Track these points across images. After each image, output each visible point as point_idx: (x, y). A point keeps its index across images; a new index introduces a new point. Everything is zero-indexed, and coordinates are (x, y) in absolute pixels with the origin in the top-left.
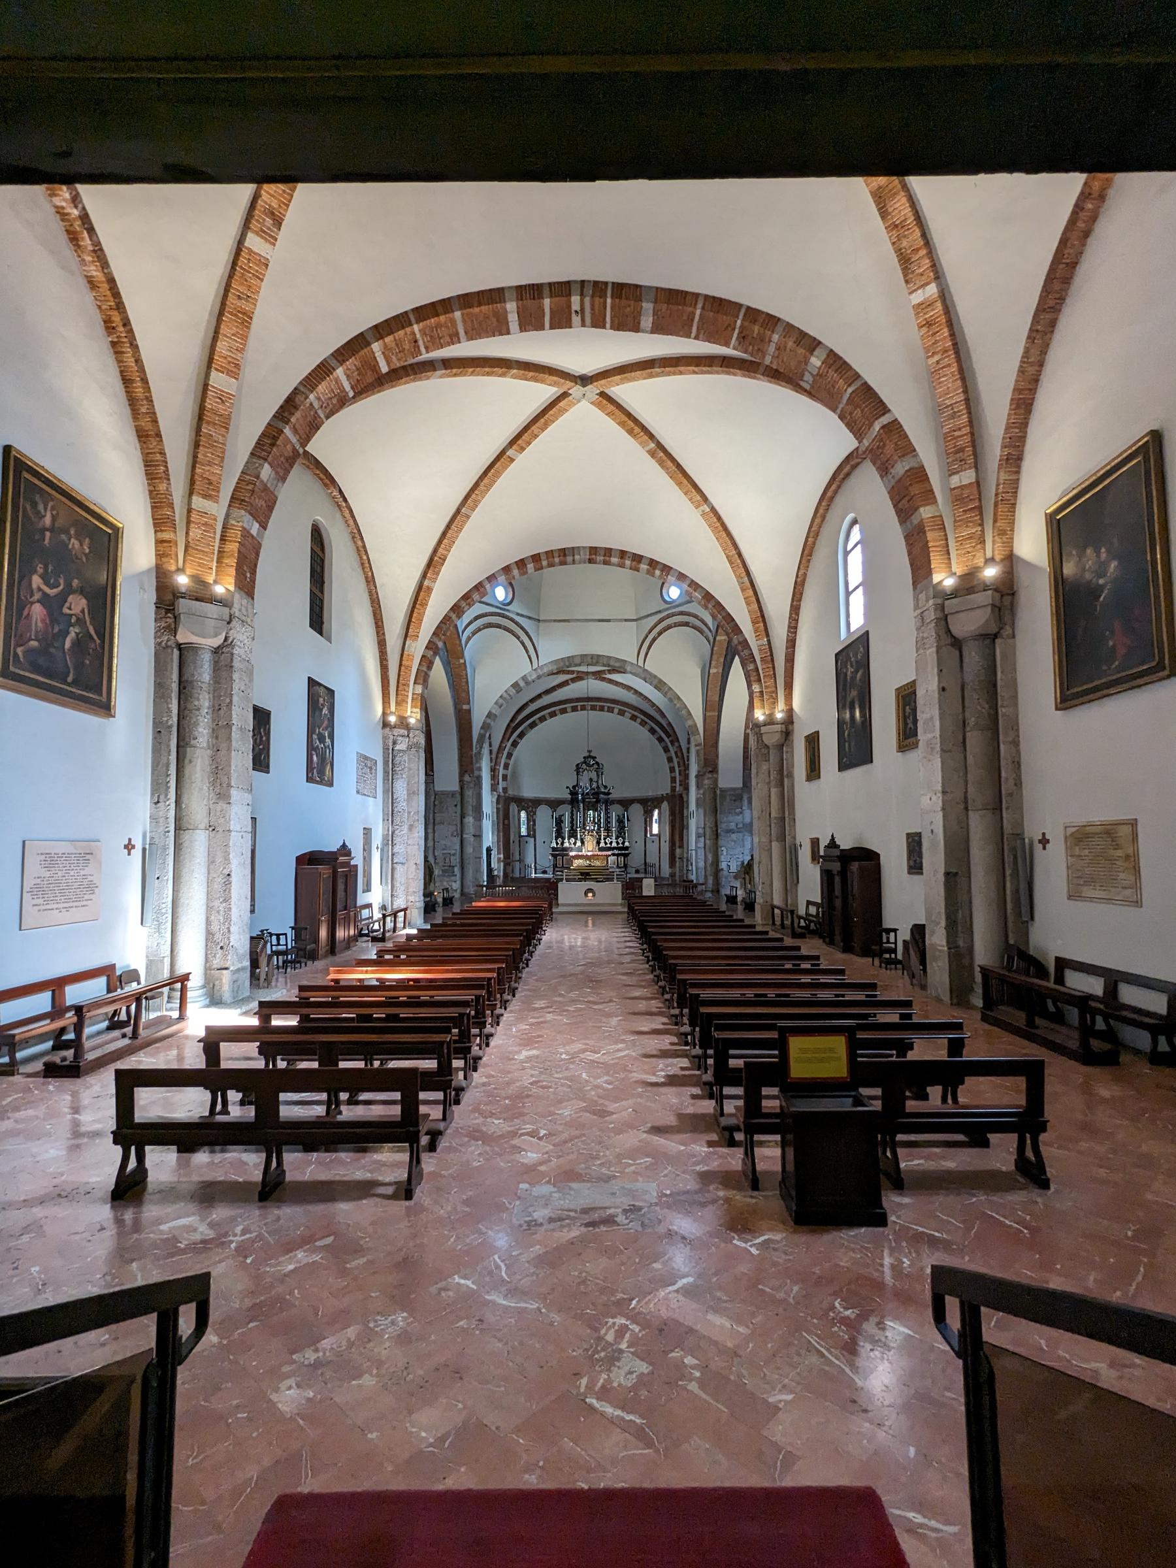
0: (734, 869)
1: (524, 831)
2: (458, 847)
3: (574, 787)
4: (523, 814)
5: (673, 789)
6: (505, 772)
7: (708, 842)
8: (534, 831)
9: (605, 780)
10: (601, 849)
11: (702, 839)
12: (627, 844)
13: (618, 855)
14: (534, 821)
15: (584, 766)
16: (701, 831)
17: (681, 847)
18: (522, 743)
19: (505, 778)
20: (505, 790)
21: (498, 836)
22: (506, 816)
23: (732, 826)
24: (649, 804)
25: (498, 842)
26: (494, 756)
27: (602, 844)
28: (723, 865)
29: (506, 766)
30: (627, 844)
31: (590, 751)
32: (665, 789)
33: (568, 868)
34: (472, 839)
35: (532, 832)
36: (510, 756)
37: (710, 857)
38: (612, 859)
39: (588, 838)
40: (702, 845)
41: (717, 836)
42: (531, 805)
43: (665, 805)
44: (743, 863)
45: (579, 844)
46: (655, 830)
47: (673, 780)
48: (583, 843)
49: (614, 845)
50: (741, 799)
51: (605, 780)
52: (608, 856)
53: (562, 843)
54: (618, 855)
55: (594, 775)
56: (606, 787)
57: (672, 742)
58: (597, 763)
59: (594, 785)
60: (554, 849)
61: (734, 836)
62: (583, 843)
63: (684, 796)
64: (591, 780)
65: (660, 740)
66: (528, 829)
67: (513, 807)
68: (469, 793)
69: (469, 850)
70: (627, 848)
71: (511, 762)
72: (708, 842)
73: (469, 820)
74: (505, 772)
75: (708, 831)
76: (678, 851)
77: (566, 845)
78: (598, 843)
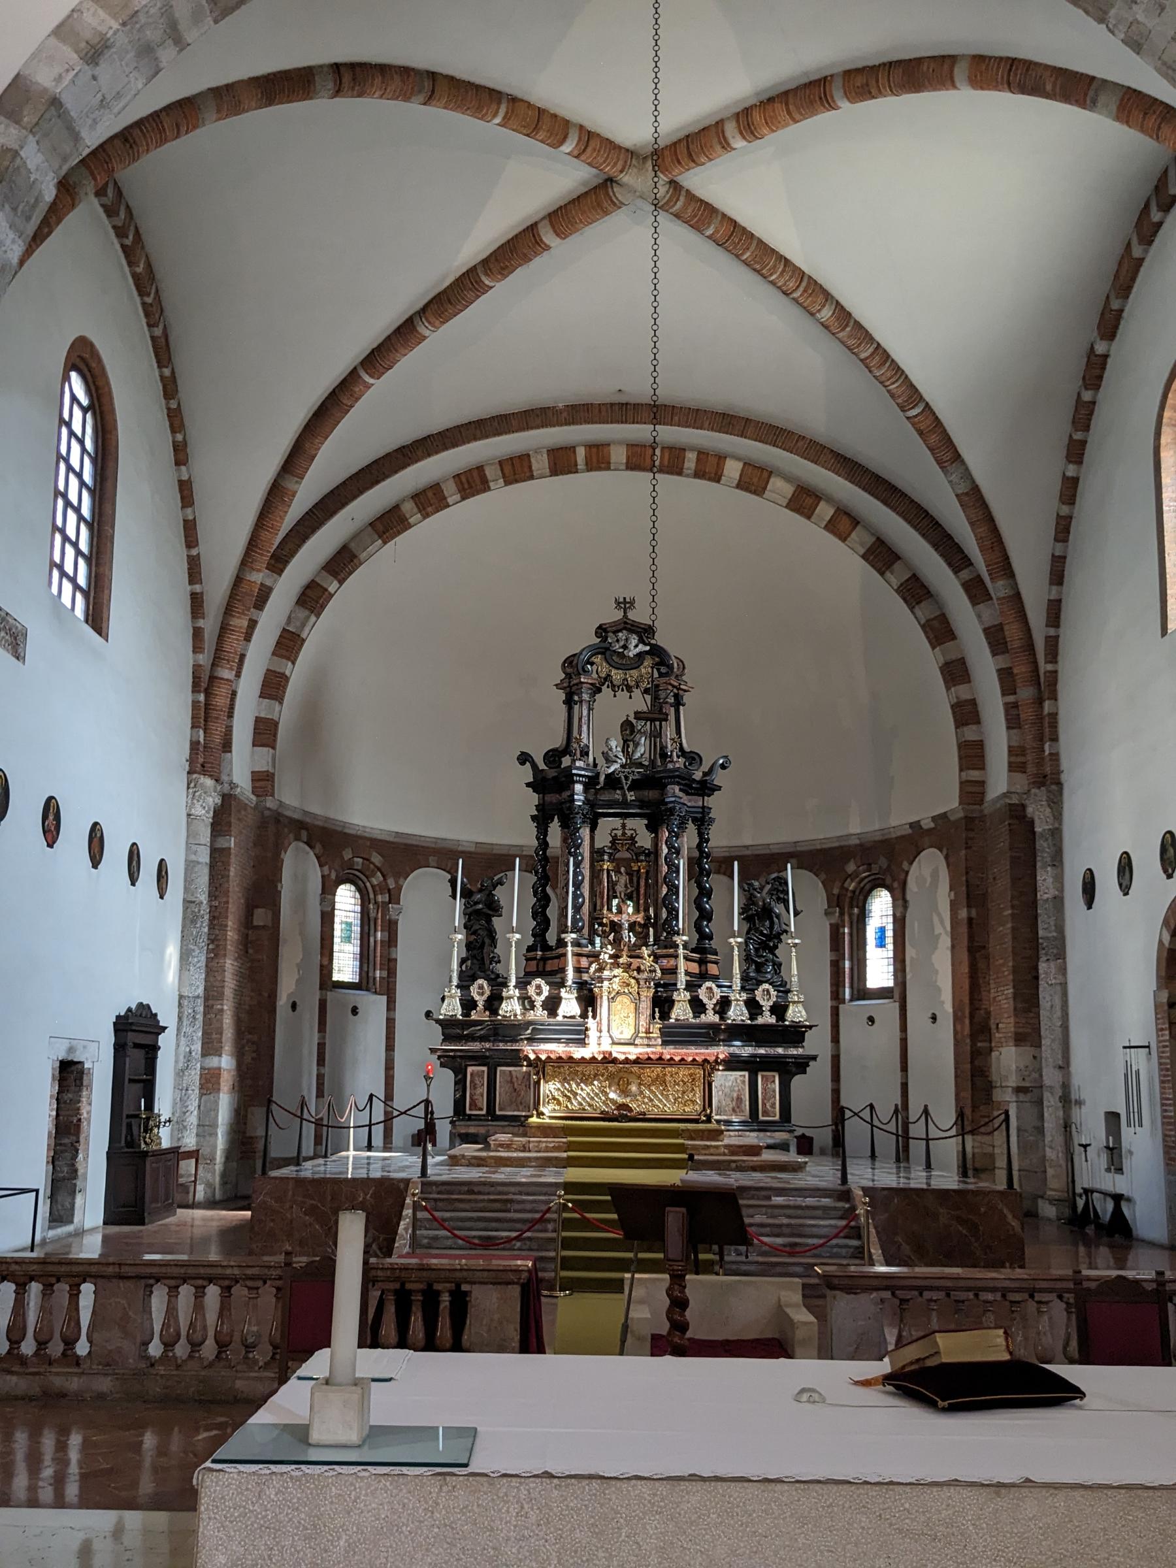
1: (345, 967)
3: (552, 757)
4: (346, 900)
6: (268, 709)
8: (390, 966)
10: (671, 1036)
13: (753, 1066)
14: (391, 928)
15: (600, 667)
17: (1029, 1036)
18: (346, 596)
19: (265, 732)
20: (263, 781)
21: (212, 971)
22: (263, 891)
25: (212, 995)
26: (210, 625)
27: (681, 1011)
29: (274, 686)
31: (625, 604)
32: (935, 794)
33: (518, 1124)
35: (379, 969)
36: (289, 644)
38: (729, 1083)
39: (613, 980)
42: (379, 865)
45: (570, 1006)
46: (879, 971)
48: (588, 1001)
49: (738, 1013)
51: (692, 731)
52: (709, 1067)
53: (493, 1003)
54: (753, 1066)
57: (976, 591)
58: (657, 652)
59: (642, 751)
60: (448, 1025)
62: (588, 1001)
65: (915, 591)
66: (365, 957)
70: (796, 1034)
71: (298, 673)
74: (268, 709)
77: (511, 1007)
78: (662, 1004)
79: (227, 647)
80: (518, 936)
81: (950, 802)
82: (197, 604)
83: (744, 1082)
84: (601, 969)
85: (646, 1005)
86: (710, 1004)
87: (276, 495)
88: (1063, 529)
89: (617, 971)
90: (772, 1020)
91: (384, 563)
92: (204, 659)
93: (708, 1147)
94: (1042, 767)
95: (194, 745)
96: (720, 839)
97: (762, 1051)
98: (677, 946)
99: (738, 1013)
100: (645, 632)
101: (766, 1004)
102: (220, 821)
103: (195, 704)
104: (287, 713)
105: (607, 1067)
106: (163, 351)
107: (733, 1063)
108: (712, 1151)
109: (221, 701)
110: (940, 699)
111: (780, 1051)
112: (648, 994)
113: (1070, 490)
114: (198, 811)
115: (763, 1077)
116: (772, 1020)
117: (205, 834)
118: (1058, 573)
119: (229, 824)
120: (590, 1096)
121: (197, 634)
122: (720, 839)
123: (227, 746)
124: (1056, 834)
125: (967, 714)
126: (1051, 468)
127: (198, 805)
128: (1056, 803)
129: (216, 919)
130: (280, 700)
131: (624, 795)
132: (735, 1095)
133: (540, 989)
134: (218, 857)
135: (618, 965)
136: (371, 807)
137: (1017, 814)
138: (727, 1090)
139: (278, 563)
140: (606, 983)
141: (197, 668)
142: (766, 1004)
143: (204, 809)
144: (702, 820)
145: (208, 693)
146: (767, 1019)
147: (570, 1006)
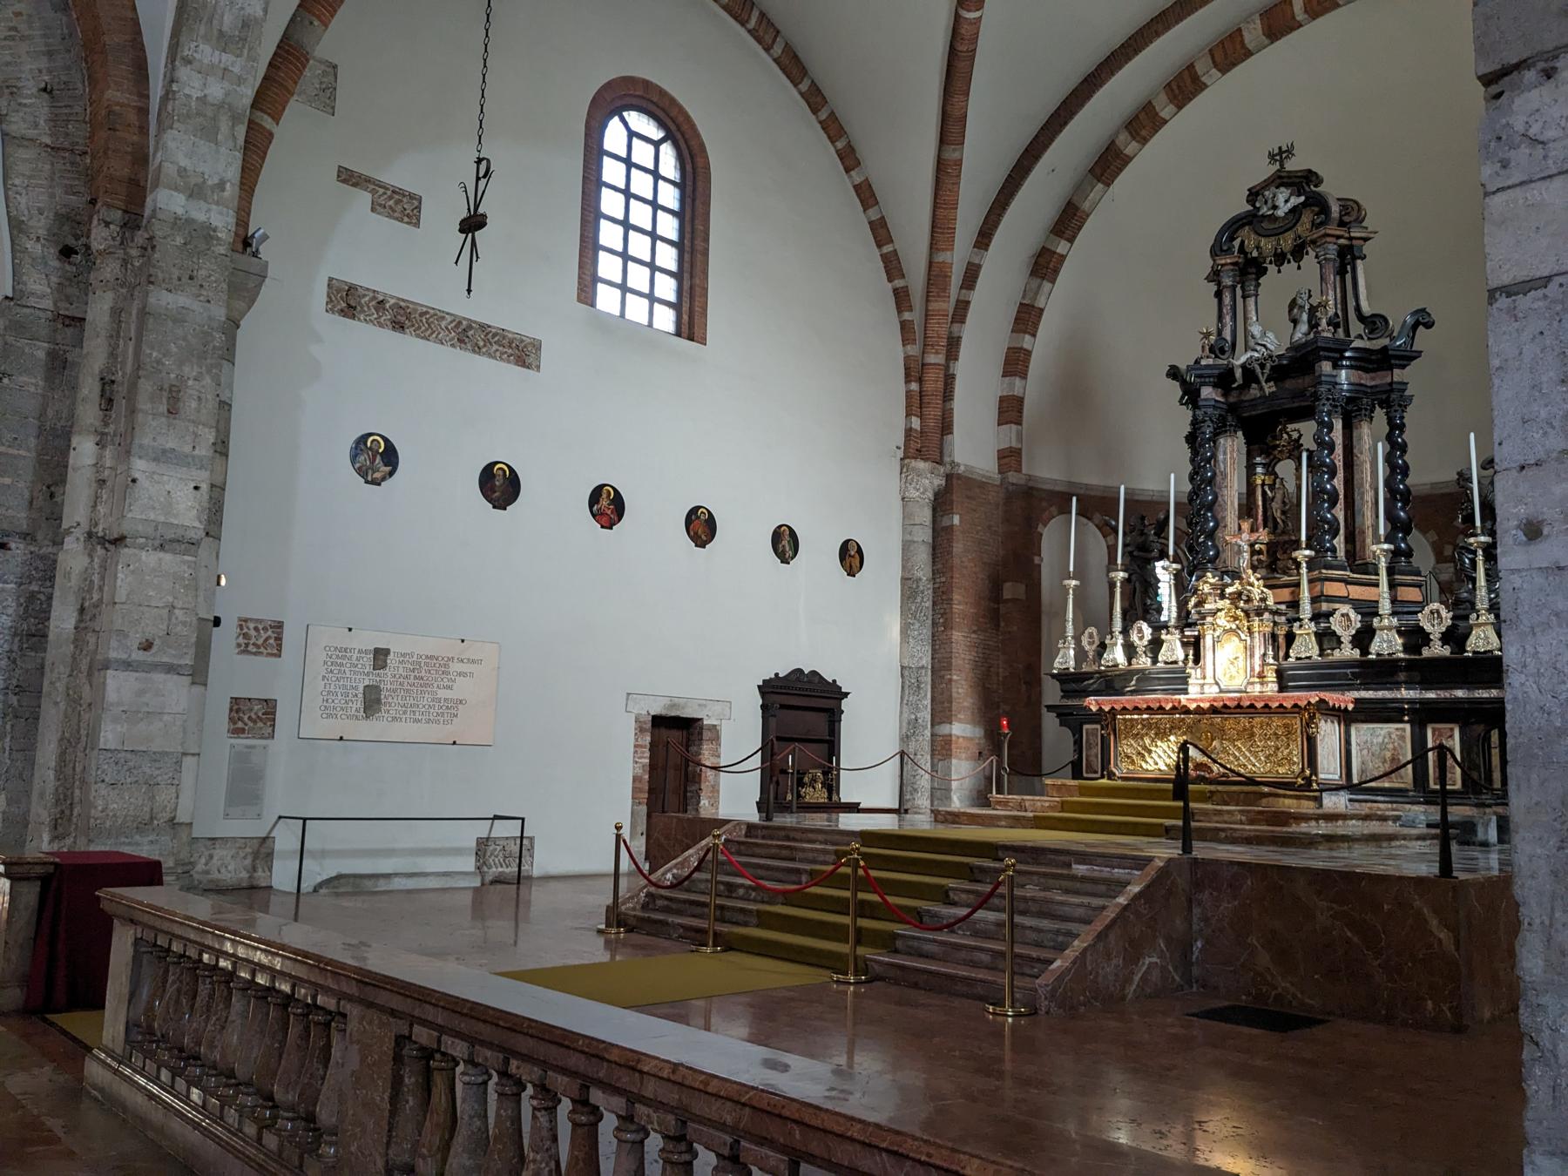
12: (1481, 639)
26: (914, 316)
49: (1387, 643)
54: (1422, 715)
70: (1490, 669)
79: (930, 334)
80: (1122, 575)
83: (1402, 738)
84: (1200, 604)
85: (1258, 641)
86: (1346, 636)
89: (1221, 604)
90: (1446, 651)
92: (914, 350)
93: (1220, 812)
95: (909, 432)
97: (1431, 695)
98: (1298, 565)
99: (1387, 643)
101: (1435, 630)
102: (941, 503)
103: (909, 394)
108: (1226, 817)
109: (934, 382)
111: (1460, 693)
112: (1262, 626)
114: (913, 493)
115: (1434, 730)
116: (1446, 651)
117: (925, 515)
119: (952, 502)
121: (905, 327)
123: (946, 427)
127: (910, 488)
129: (941, 597)
130: (1024, 375)
131: (1261, 389)
132: (1388, 755)
133: (1143, 632)
135: (1222, 596)
138: (1376, 749)
140: (1209, 619)
141: (907, 358)
142: (1435, 630)
145: (920, 381)
146: (1437, 650)
147: (1173, 648)
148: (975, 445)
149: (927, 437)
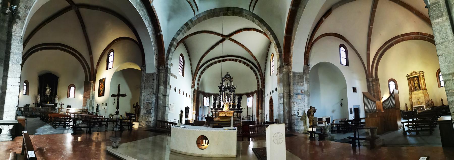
0: (300, 115)
2: (154, 100)
5: (258, 88)
7: (285, 100)
9: (233, 83)
10: (231, 109)
11: (282, 99)
16: (281, 95)
17: (262, 109)
19: (198, 84)
20: (198, 88)
21: (194, 104)
23: (299, 91)
24: (249, 95)
25: (193, 106)
27: (231, 108)
28: (294, 112)
29: (199, 80)
30: (241, 108)
31: (228, 73)
34: (162, 97)
36: (200, 77)
37: (287, 109)
40: (282, 102)
41: (290, 97)
43: (255, 95)
44: (304, 111)
47: (258, 85)
50: (303, 78)
51: (233, 83)
55: (229, 82)
56: (233, 86)
57: (259, 71)
58: (230, 77)
61: (300, 97)
63: (263, 90)
64: (228, 84)
67: (201, 96)
68: (162, 75)
69: (161, 102)
71: (201, 79)
72: (285, 100)
73: (162, 87)
75: (286, 95)
76: (260, 111)
78: (230, 107)
81: (257, 89)
82: (192, 73)
87: (198, 64)
88: (265, 66)
91: (208, 70)
94: (263, 86)
96: (235, 93)
100: (229, 75)
102: (194, 92)
104: (200, 82)
105: (226, 112)
106: (189, 53)
107: (236, 112)
110: (256, 80)
113: (266, 63)
118: (265, 70)
120: (224, 115)
122: (235, 93)
124: (264, 92)
125: (258, 82)
126: (264, 61)
128: (264, 89)
134: (194, 94)
136: (207, 91)
137: (261, 90)
139: (199, 70)
143: (193, 91)
144: (234, 91)
148: (196, 87)
149: (193, 86)
